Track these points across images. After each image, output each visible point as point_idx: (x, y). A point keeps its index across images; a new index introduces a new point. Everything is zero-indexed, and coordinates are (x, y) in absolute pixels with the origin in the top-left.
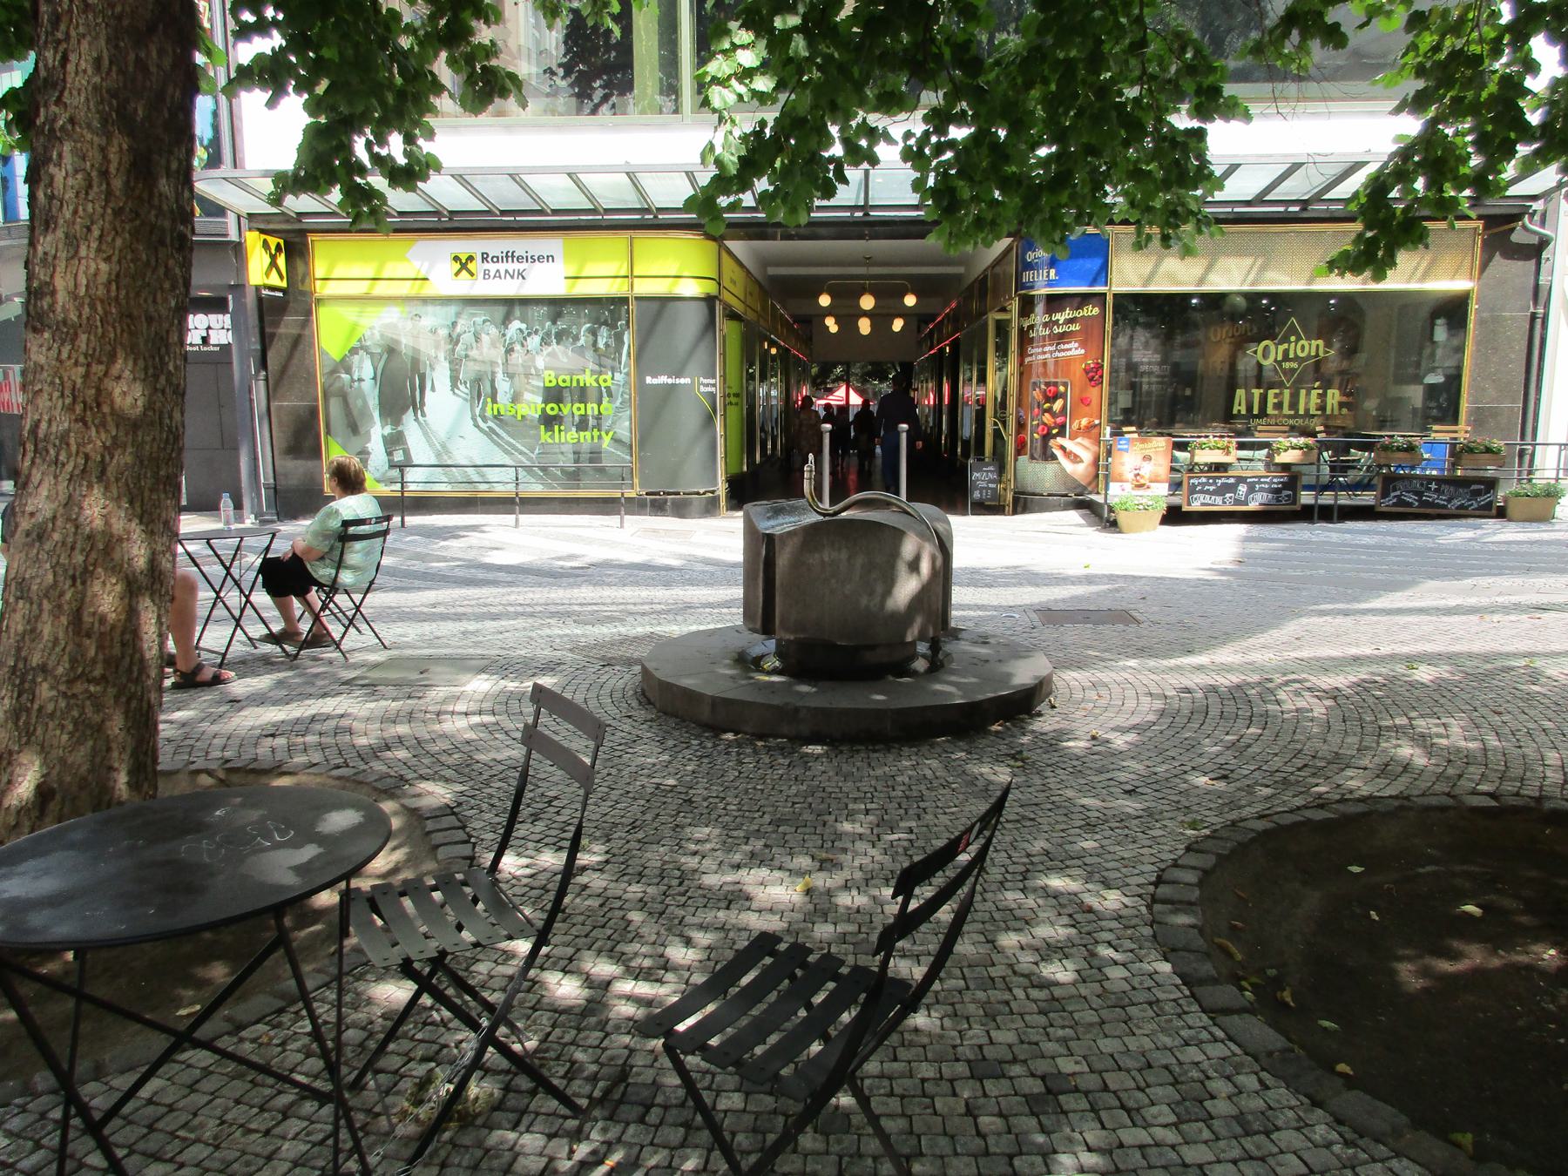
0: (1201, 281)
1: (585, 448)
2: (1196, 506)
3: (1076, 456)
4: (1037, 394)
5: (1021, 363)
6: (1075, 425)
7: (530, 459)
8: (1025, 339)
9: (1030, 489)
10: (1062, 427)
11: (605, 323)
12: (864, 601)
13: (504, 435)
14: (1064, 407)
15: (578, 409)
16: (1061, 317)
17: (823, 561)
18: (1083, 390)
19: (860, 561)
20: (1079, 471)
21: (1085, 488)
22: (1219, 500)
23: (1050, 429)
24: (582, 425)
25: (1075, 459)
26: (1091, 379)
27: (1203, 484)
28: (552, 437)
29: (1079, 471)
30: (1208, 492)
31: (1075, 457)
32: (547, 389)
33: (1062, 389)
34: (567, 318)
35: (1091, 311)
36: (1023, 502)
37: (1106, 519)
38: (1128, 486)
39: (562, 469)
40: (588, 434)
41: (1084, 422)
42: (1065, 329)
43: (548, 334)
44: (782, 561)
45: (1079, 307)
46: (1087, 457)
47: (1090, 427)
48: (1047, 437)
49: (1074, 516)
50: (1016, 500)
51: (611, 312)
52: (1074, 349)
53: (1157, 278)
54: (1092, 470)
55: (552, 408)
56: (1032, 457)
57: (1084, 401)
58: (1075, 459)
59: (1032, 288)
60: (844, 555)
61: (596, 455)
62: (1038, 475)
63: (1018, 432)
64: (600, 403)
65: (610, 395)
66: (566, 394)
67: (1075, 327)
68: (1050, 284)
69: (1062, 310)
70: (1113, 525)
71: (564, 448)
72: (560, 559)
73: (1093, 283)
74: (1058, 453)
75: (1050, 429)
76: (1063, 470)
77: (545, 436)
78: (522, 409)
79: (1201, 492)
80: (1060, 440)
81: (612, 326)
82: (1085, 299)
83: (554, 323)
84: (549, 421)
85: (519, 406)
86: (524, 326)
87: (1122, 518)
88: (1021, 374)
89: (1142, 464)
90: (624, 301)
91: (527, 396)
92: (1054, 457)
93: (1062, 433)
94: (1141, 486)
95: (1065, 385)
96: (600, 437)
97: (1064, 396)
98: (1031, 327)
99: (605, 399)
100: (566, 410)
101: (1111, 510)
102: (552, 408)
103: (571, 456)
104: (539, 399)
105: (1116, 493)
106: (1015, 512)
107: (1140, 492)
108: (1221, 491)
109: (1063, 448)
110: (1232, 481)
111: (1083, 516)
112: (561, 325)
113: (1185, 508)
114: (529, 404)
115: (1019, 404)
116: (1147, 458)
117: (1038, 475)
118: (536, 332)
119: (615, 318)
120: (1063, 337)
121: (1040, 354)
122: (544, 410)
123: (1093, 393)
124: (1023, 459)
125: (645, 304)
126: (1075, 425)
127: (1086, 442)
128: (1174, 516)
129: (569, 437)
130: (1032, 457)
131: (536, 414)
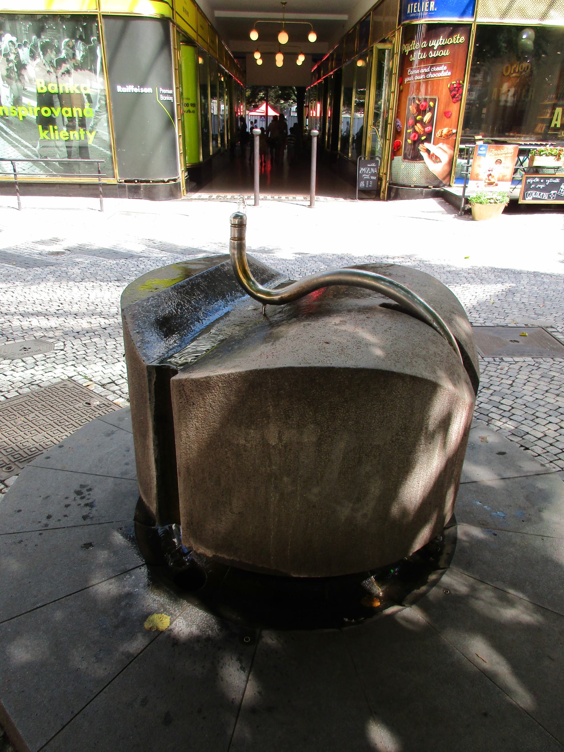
0: (544, 16)
1: (75, 144)
2: (529, 200)
3: (437, 157)
4: (412, 108)
5: (401, 82)
6: (438, 134)
7: (32, 151)
8: (405, 61)
9: (401, 182)
10: (429, 135)
11: (81, 38)
12: (344, 512)
13: (11, 133)
14: (432, 118)
15: (67, 112)
16: (435, 44)
17: (265, 444)
18: (447, 105)
19: (341, 445)
20: (438, 169)
21: (441, 182)
22: (546, 195)
23: (420, 136)
24: (71, 125)
25: (436, 159)
26: (453, 97)
27: (536, 183)
28: (48, 134)
29: (438, 169)
30: (539, 189)
31: (437, 157)
32: (40, 95)
33: (431, 104)
34: (49, 32)
35: (459, 39)
36: (396, 191)
37: (462, 208)
38: (482, 184)
39: (61, 163)
40: (76, 133)
41: (445, 131)
42: (438, 54)
43: (35, 46)
44: (191, 435)
45: (451, 35)
46: (445, 159)
47: (449, 135)
48: (417, 142)
49: (433, 204)
50: (390, 189)
51: (84, 27)
52: (443, 71)
53: (511, 12)
54: (447, 168)
55: (46, 112)
56: (405, 158)
57: (447, 114)
58: (436, 159)
59: (416, 17)
60: (309, 436)
61: (83, 150)
62: (409, 171)
63: (395, 138)
64: (83, 107)
65: (90, 101)
66: (56, 100)
67: (446, 53)
68: (431, 14)
69: (437, 37)
70: (468, 213)
71: (59, 144)
72: (43, 242)
73: (463, 14)
74: (424, 154)
75: (420, 136)
76: (427, 168)
77: (43, 135)
78: (22, 112)
79: (535, 189)
80: (426, 145)
81: (86, 41)
82: (455, 28)
83: (39, 36)
84: (46, 122)
85: (19, 109)
86: (14, 39)
87: (477, 209)
88: (401, 92)
89: (494, 166)
90: (92, 18)
91: (25, 100)
92: (421, 158)
93: (428, 140)
94: (491, 184)
95: (434, 100)
96: (85, 135)
97: (432, 110)
98: (411, 52)
99: (87, 105)
100: (57, 112)
101: (467, 201)
102: (46, 112)
103: (65, 150)
104: (34, 103)
105: (474, 190)
106: (389, 198)
107: (491, 188)
108: (547, 189)
109: (428, 151)
110: (557, 181)
111: (440, 203)
112: (45, 38)
113: (521, 202)
114: (27, 107)
115: (398, 115)
116: (499, 162)
117: (409, 171)
118: (25, 44)
119: (88, 32)
120: (436, 60)
121: (416, 74)
122: (39, 112)
123: (454, 108)
124: (398, 159)
125: (112, 21)
126: (438, 134)
127: (445, 147)
128: (514, 207)
129: (60, 135)
130: (405, 158)
131: (33, 116)
